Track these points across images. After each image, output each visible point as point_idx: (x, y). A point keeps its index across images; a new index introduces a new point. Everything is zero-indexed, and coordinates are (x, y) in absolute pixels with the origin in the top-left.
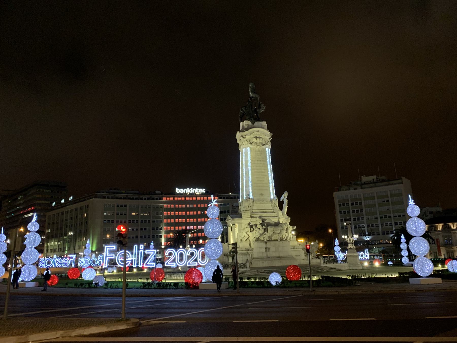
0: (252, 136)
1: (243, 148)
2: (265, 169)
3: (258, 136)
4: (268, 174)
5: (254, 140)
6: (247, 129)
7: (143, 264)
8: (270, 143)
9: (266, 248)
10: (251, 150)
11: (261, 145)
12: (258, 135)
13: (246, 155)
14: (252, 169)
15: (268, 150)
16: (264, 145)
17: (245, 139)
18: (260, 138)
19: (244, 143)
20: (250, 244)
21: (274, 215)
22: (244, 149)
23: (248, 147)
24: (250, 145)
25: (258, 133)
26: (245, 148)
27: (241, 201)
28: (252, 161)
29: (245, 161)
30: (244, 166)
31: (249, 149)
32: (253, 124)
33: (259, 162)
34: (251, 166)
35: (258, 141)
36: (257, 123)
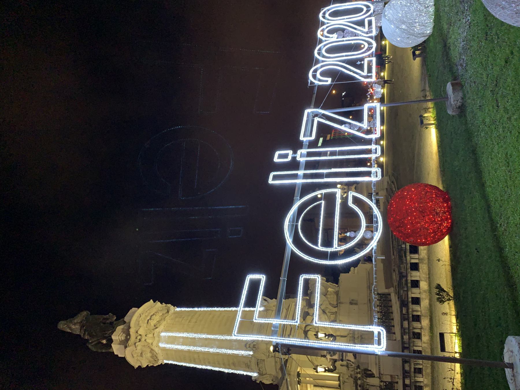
0: (144, 325)
1: (158, 346)
2: (210, 314)
3: (149, 318)
4: (219, 311)
5: (152, 323)
6: (128, 334)
7: (369, 142)
8: (169, 305)
9: (351, 303)
10: (166, 331)
11: (167, 314)
12: (146, 316)
13: (173, 340)
14: (201, 332)
15: (178, 309)
16: (168, 312)
17: (143, 340)
18: (154, 314)
19: (149, 341)
20: (342, 336)
21: (293, 306)
22: (162, 345)
23: (159, 336)
24: (157, 329)
25: (143, 316)
26: (159, 341)
27: (255, 375)
28: (187, 331)
29: (183, 344)
30: (192, 348)
31: (163, 334)
32: (125, 322)
33: (194, 320)
34: (196, 332)
35: (156, 318)
36: (126, 319)
